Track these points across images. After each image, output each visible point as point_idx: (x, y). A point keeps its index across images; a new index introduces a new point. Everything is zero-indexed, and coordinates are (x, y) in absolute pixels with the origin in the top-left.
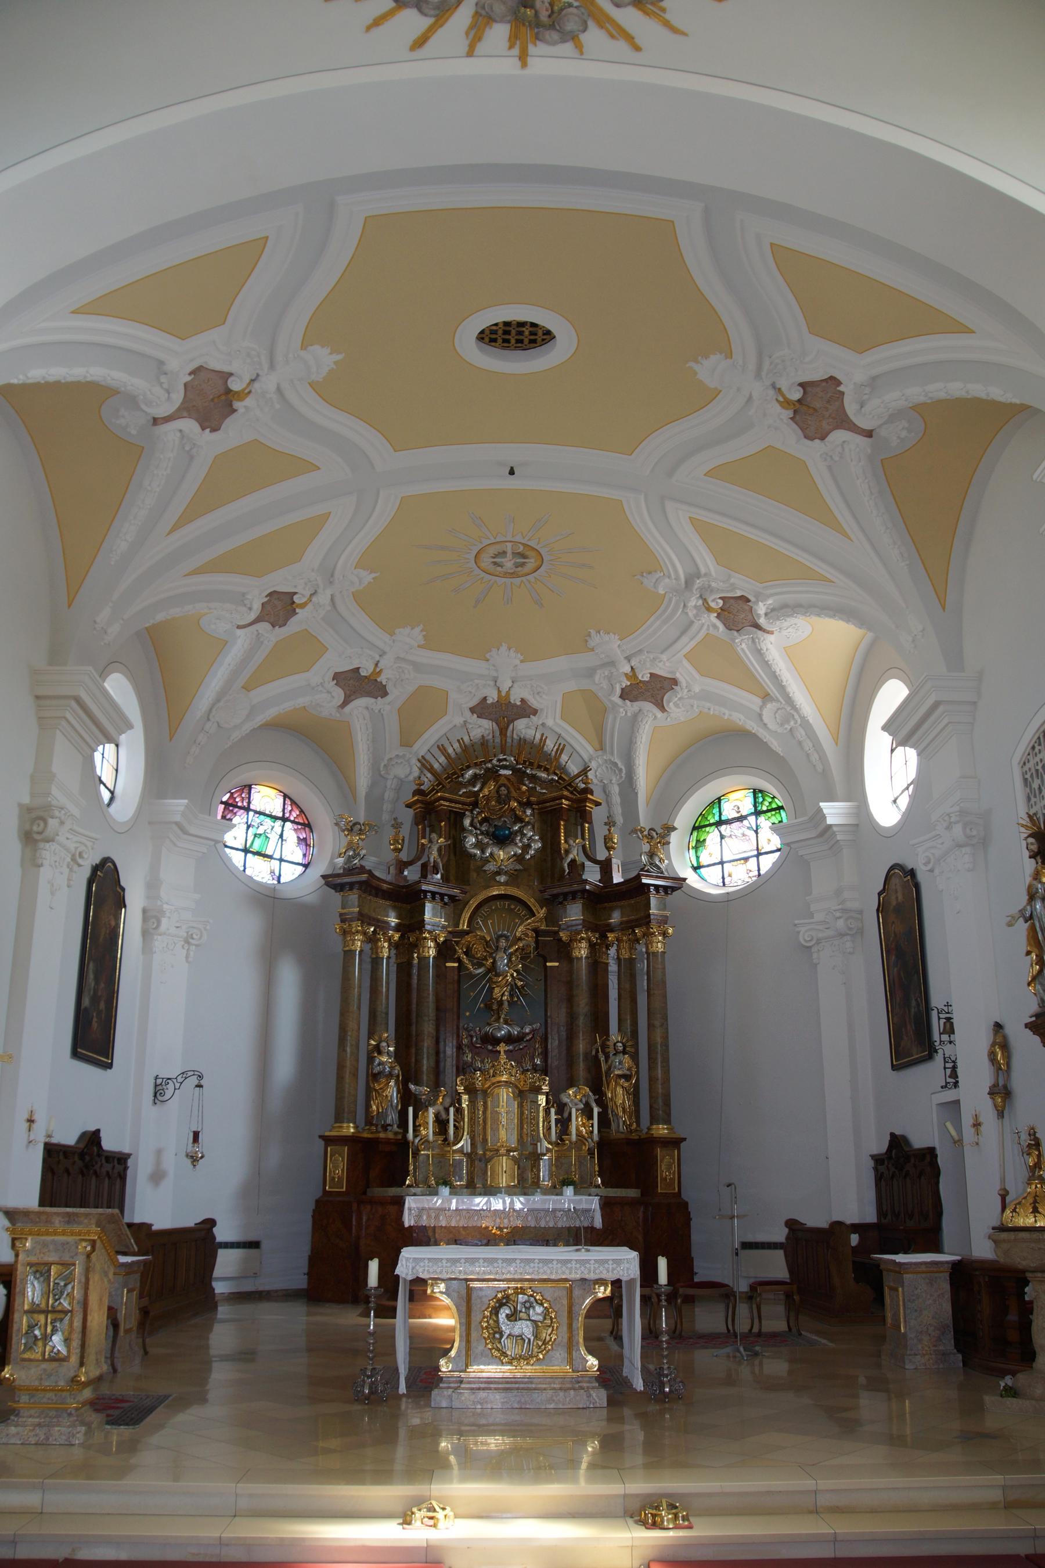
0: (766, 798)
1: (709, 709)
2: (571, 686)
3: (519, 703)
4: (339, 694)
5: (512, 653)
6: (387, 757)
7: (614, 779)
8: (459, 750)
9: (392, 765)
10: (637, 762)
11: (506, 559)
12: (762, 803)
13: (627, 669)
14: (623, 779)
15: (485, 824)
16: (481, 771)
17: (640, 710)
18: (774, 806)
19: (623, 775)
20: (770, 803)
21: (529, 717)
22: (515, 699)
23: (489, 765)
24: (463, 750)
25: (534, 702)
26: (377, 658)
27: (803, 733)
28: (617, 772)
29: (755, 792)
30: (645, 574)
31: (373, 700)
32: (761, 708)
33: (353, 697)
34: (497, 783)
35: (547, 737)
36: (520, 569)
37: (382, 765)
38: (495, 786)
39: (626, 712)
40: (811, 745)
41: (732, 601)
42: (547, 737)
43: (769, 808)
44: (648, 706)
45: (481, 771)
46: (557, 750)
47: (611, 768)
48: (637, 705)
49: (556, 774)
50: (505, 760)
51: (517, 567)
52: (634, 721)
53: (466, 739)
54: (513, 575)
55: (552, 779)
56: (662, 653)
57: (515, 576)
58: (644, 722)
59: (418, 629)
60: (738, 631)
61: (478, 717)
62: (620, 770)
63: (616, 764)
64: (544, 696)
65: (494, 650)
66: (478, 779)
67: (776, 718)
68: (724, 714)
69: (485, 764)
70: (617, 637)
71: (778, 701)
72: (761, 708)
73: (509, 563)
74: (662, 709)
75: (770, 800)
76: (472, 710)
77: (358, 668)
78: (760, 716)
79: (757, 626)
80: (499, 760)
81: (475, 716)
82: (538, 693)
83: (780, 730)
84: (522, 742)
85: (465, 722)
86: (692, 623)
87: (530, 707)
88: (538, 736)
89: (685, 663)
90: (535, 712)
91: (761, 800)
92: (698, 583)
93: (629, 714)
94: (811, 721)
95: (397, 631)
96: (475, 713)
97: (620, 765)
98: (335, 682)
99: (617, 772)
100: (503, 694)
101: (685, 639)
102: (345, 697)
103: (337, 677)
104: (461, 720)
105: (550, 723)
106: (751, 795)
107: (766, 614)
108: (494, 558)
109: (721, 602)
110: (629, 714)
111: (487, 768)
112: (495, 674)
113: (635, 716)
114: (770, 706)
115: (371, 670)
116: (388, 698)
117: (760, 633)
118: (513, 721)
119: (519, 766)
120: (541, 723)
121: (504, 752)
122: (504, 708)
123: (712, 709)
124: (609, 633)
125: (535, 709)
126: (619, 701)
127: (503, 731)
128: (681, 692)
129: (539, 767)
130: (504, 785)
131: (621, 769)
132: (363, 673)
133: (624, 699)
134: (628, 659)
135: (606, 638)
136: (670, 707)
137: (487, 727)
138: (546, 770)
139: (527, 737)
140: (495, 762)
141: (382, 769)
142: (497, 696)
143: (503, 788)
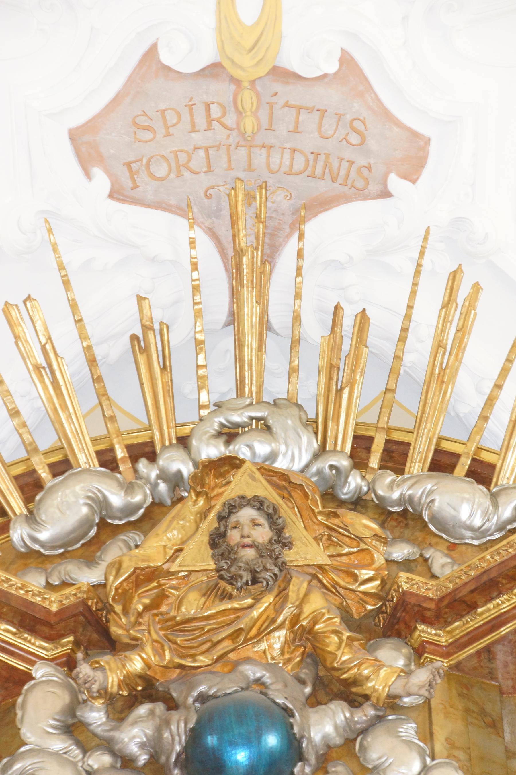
15: (143, 710)
21: (386, 194)
35: (477, 288)
42: (477, 288)
66: (117, 530)
111: (163, 476)
125: (415, 135)
142: (211, 21)
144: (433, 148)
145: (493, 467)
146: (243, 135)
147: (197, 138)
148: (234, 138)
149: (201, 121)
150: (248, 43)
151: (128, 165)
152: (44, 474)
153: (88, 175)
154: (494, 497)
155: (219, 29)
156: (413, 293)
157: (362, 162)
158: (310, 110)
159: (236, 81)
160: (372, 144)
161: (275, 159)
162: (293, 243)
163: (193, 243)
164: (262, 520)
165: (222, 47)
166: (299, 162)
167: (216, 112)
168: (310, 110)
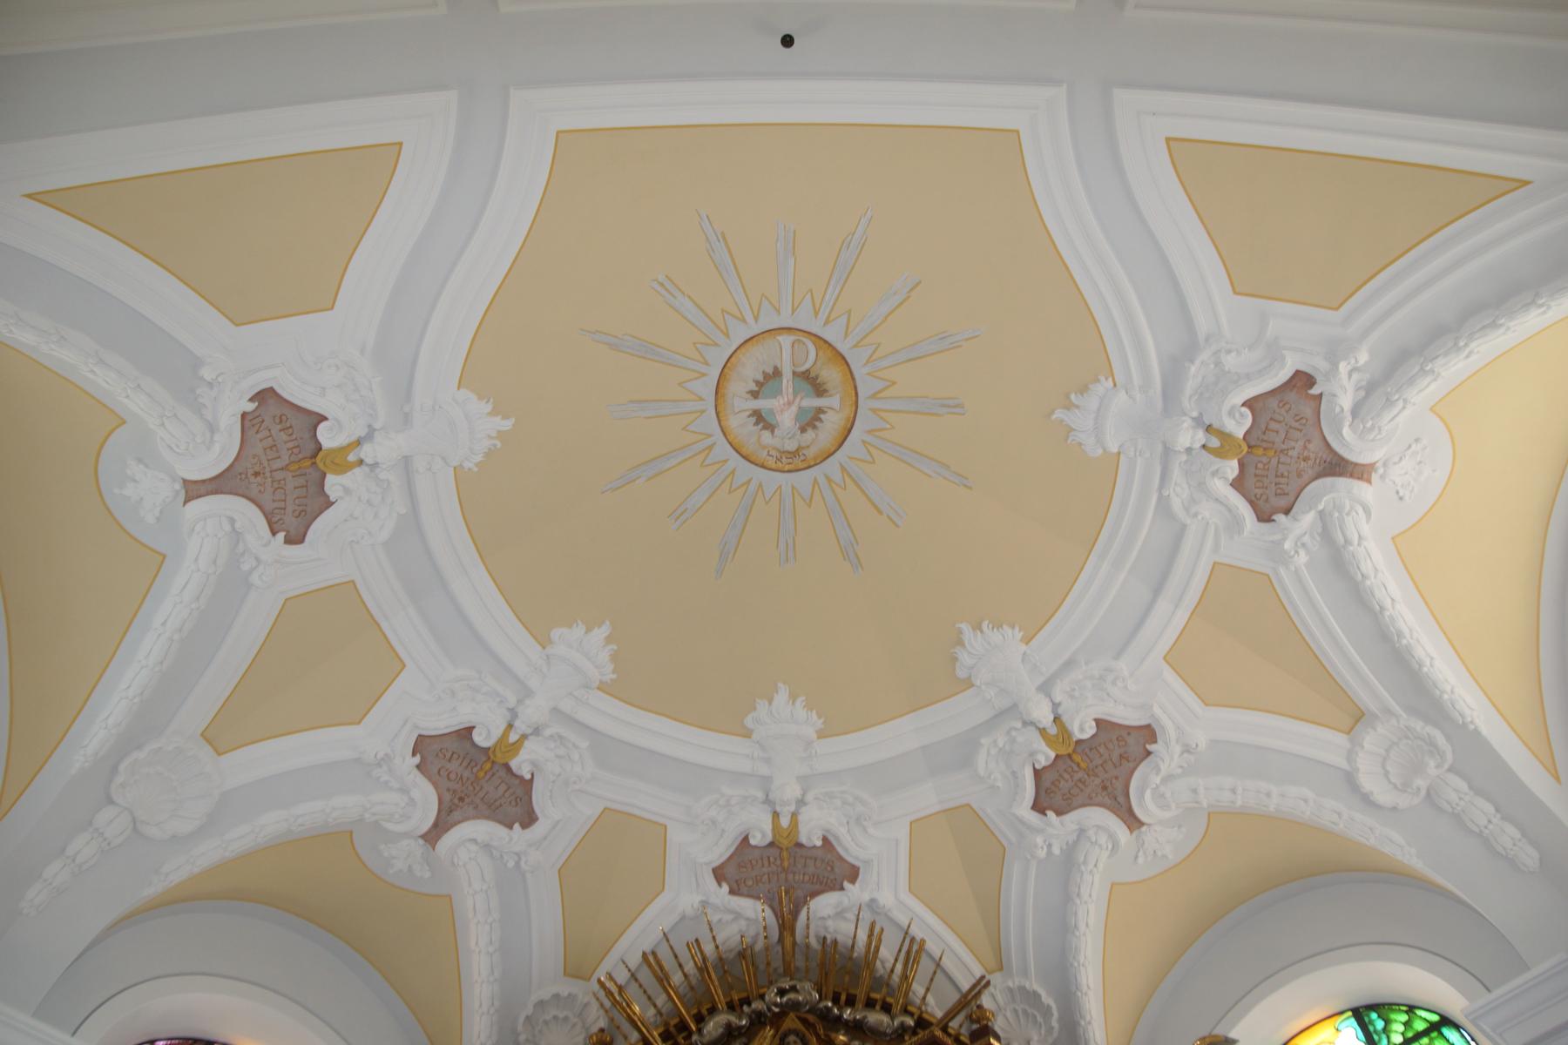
0: (1393, 1016)
1: (1234, 791)
2: (927, 798)
3: (819, 843)
4: (425, 799)
5: (800, 711)
6: (534, 998)
7: (1036, 1038)
8: (690, 967)
9: (546, 1023)
10: (1083, 981)
11: (782, 400)
12: (1386, 1030)
13: (1044, 716)
14: (1055, 1034)
16: (740, 1018)
17: (1082, 832)
18: (1420, 1026)
19: (1055, 1024)
20: (1407, 1024)
21: (842, 889)
22: (810, 835)
23: (757, 1005)
24: (700, 970)
25: (852, 847)
26: (512, 702)
27: (1463, 786)
28: (1040, 1019)
29: (1359, 1014)
30: (1073, 397)
31: (501, 831)
32: (1350, 756)
33: (456, 815)
34: (777, 1032)
35: (882, 930)
36: (810, 434)
37: (521, 1020)
38: (774, 1036)
39: (1050, 846)
40: (1490, 808)
41: (1273, 403)
43: (1410, 1034)
44: (1097, 818)
45: (740, 1018)
46: (908, 953)
47: (1025, 1012)
48: (1072, 818)
49: (911, 1014)
50: (793, 989)
51: (803, 430)
52: (1068, 864)
53: (709, 948)
54: (794, 461)
55: (902, 1025)
56: (1117, 657)
57: (798, 463)
58: (1091, 866)
59: (601, 632)
60: (1287, 512)
61: (732, 892)
62: (1047, 1012)
63: (1036, 995)
64: (871, 830)
65: (762, 706)
67: (1386, 774)
68: (1268, 795)
69: (749, 1004)
70: (1019, 635)
71: (1389, 712)
72: (1350, 756)
73: (785, 408)
74: (1133, 821)
75: (1404, 1018)
76: (719, 874)
77: (469, 730)
78: (1350, 779)
79: (1337, 466)
80: (782, 992)
81: (725, 888)
82: (858, 820)
83: (1403, 801)
84: (830, 947)
85: (704, 904)
86: (1184, 527)
87: (841, 858)
88: (862, 936)
89: (1169, 675)
90: (853, 874)
91: (1380, 1024)
92: (1195, 374)
93: (1056, 850)
94: (1484, 731)
95: (556, 633)
96: (725, 880)
97: (1047, 1000)
98: (417, 759)
99: (1040, 1019)
100: (785, 822)
101: (1163, 606)
102: (439, 811)
103: (422, 745)
104: (696, 899)
105: (886, 898)
106: (1353, 1021)
107: (1355, 411)
108: (755, 395)
109: (1246, 410)
110: (1056, 850)
111: (754, 1011)
112: (764, 770)
113: (1070, 851)
114: (1372, 740)
115: (497, 733)
116: (538, 829)
117: (1342, 482)
118: (805, 902)
119: (821, 1005)
120: (866, 897)
121: (788, 972)
122: (786, 864)
123: (1240, 791)
124: (1000, 626)
125: (853, 866)
126: (1033, 818)
127: (786, 925)
128: (1167, 755)
129: (870, 1004)
130: (796, 1033)
131: (1049, 1007)
132: (480, 738)
133: (1042, 812)
134: (1045, 688)
135: (995, 637)
136: (1144, 804)
137: (750, 914)
138: (887, 1008)
139: (840, 938)
140: (771, 995)
141: (520, 1028)
142: (770, 827)
143: (792, 1038)
144: (861, 870)
145: (891, 1005)
146: (783, 868)
147: (765, 870)
148: (780, 869)
149: (766, 863)
150: (786, 834)
151: (737, 881)
152: (704, 1012)
153: (720, 885)
154: (892, 1019)
155: (773, 830)
156: (856, 928)
157: (832, 877)
158: (811, 858)
159: (781, 849)
160: (836, 870)
161: (797, 877)
162: (805, 909)
163: (763, 911)
164: (798, 1041)
165: (774, 836)
166: (807, 878)
167: (772, 859)
168: (811, 858)
